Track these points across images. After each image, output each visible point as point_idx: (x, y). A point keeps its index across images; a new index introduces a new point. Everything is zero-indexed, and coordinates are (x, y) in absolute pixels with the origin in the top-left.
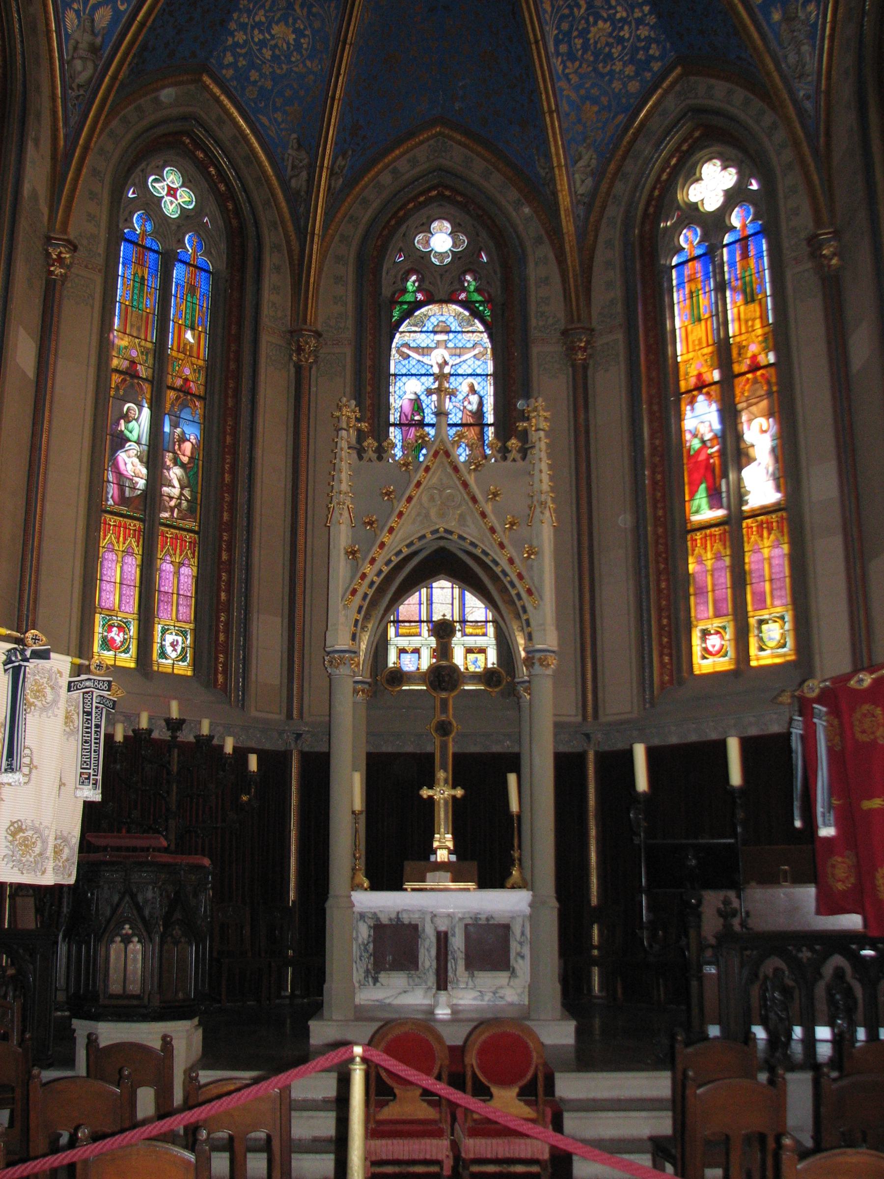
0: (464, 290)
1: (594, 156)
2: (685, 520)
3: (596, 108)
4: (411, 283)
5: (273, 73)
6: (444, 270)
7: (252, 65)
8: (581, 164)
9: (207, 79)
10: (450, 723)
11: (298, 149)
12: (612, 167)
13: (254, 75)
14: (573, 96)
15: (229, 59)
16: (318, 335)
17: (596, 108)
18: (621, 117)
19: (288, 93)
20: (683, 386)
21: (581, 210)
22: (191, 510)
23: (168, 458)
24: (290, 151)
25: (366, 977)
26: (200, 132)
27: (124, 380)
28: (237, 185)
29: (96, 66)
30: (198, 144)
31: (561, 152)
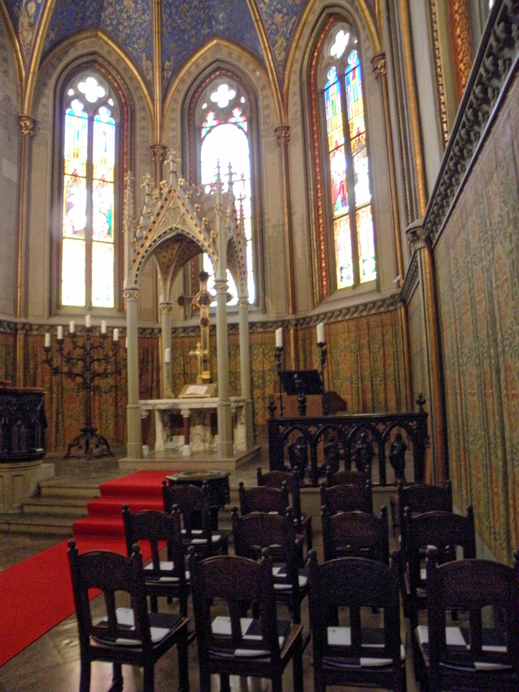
0: (233, 117)
1: (285, 41)
2: (333, 215)
3: (281, 15)
4: (211, 116)
5: (129, 25)
6: (223, 110)
7: (120, 23)
8: (278, 45)
9: (100, 34)
10: (207, 320)
11: (147, 60)
12: (294, 45)
13: (121, 28)
14: (269, 11)
15: (108, 22)
16: (164, 148)
17: (281, 15)
18: (294, 18)
19: (137, 34)
20: (330, 150)
21: (280, 68)
22: (109, 233)
23: (95, 210)
24: (144, 62)
25: (167, 438)
26: (100, 60)
27: (72, 178)
28: (121, 82)
29: (33, 33)
30: (102, 66)
31: (265, 40)
